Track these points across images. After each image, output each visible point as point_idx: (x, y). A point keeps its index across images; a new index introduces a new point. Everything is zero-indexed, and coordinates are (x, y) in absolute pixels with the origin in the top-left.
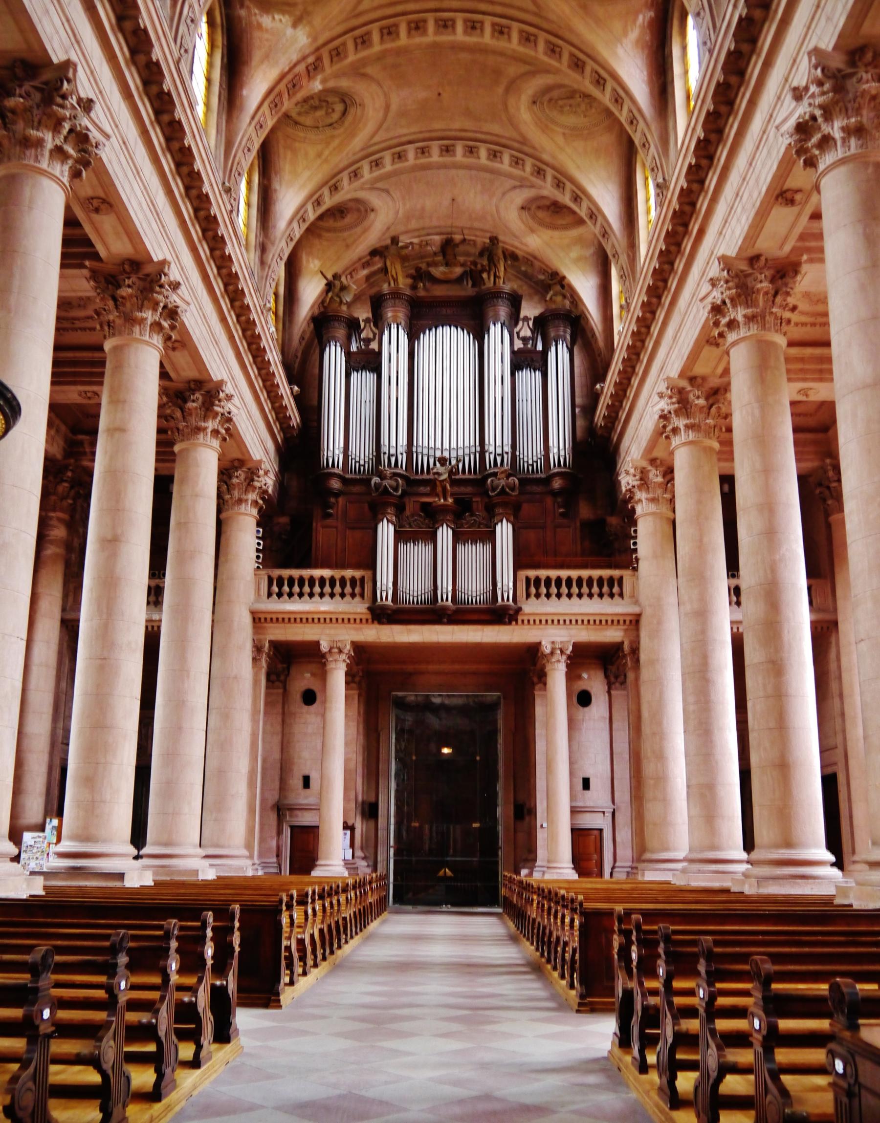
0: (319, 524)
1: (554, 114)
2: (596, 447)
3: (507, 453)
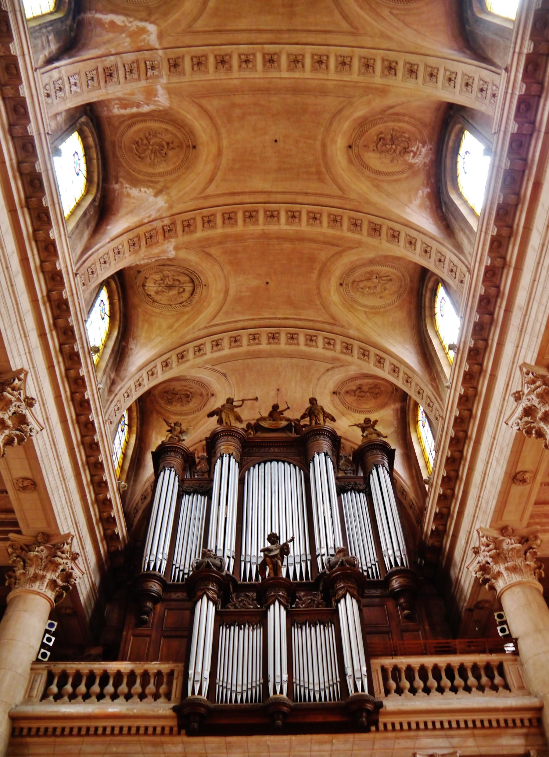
0: (130, 632)
1: (358, 297)
2: (429, 555)
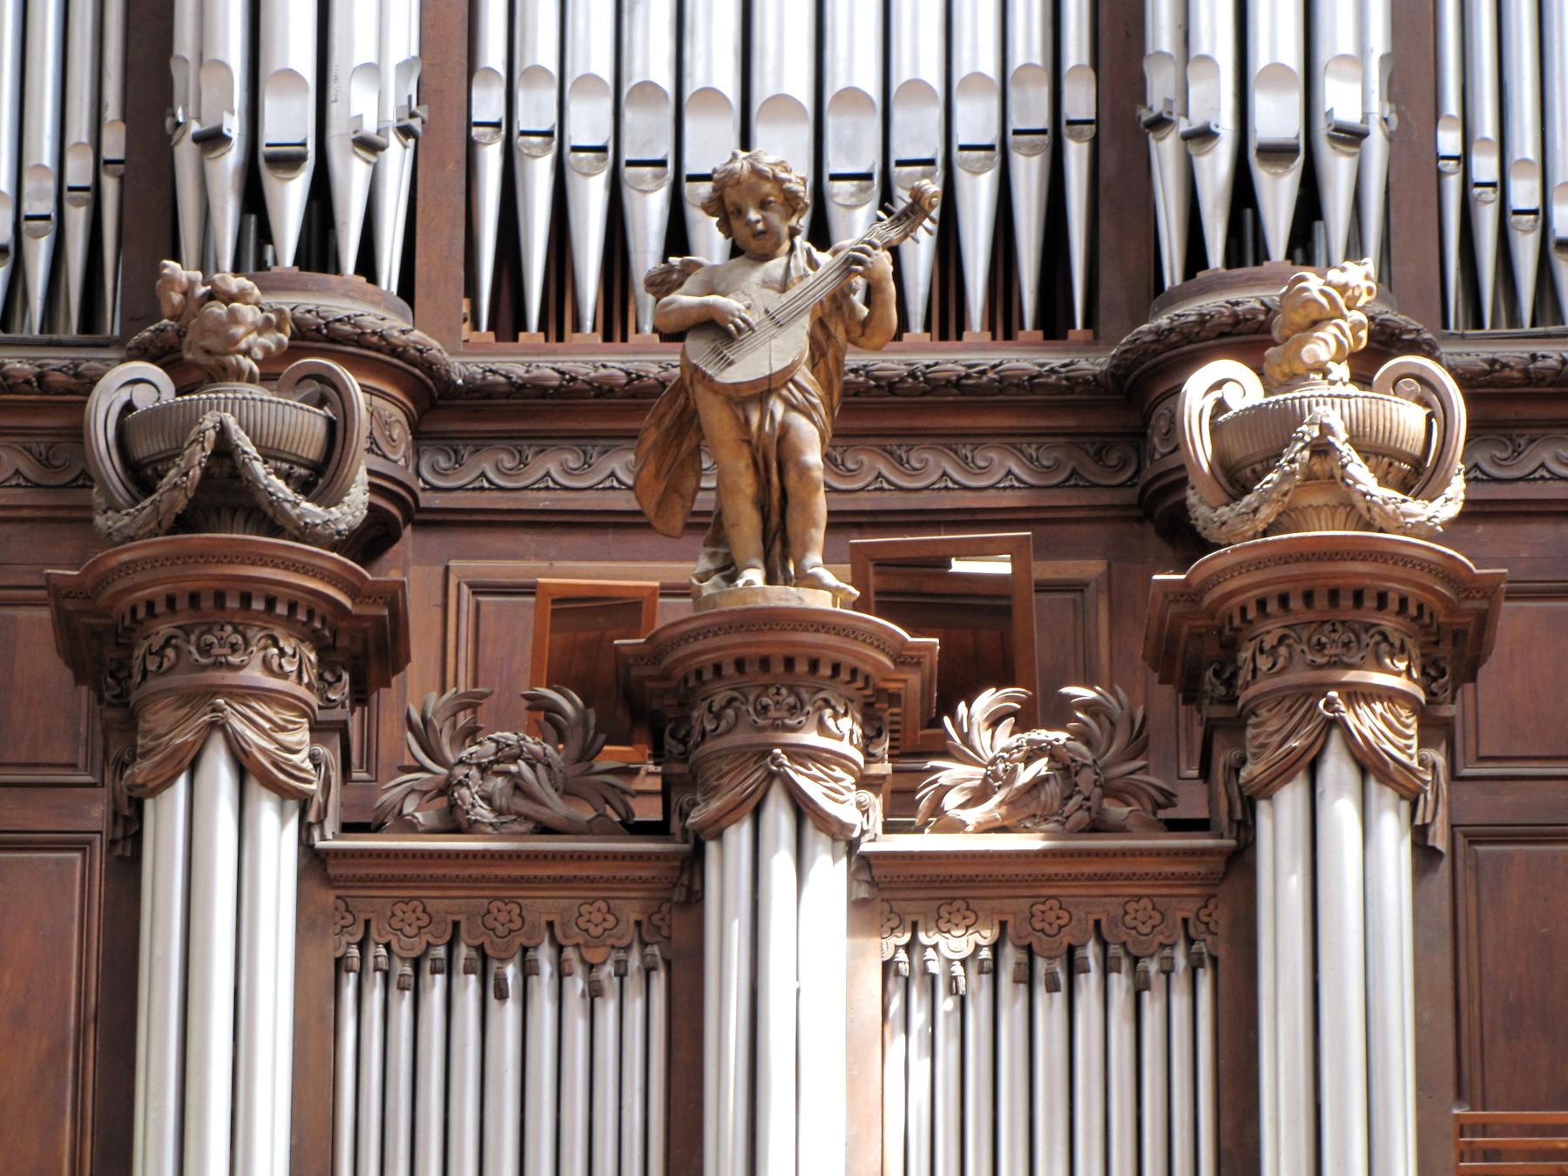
3: (1352, 137)
